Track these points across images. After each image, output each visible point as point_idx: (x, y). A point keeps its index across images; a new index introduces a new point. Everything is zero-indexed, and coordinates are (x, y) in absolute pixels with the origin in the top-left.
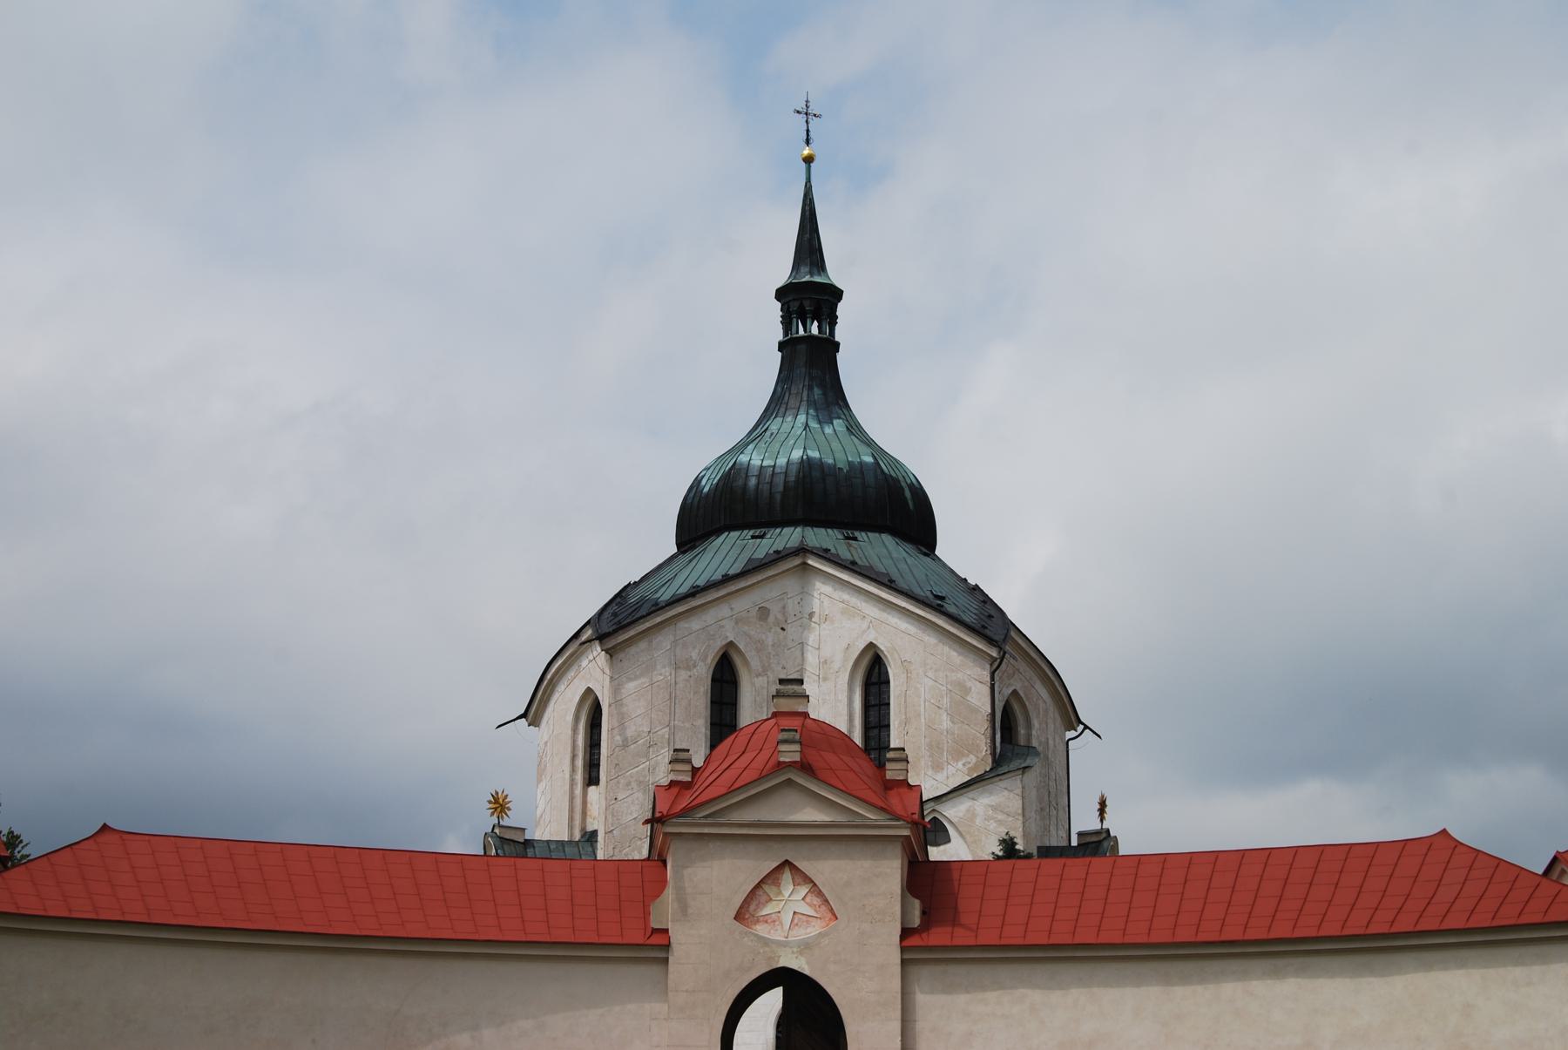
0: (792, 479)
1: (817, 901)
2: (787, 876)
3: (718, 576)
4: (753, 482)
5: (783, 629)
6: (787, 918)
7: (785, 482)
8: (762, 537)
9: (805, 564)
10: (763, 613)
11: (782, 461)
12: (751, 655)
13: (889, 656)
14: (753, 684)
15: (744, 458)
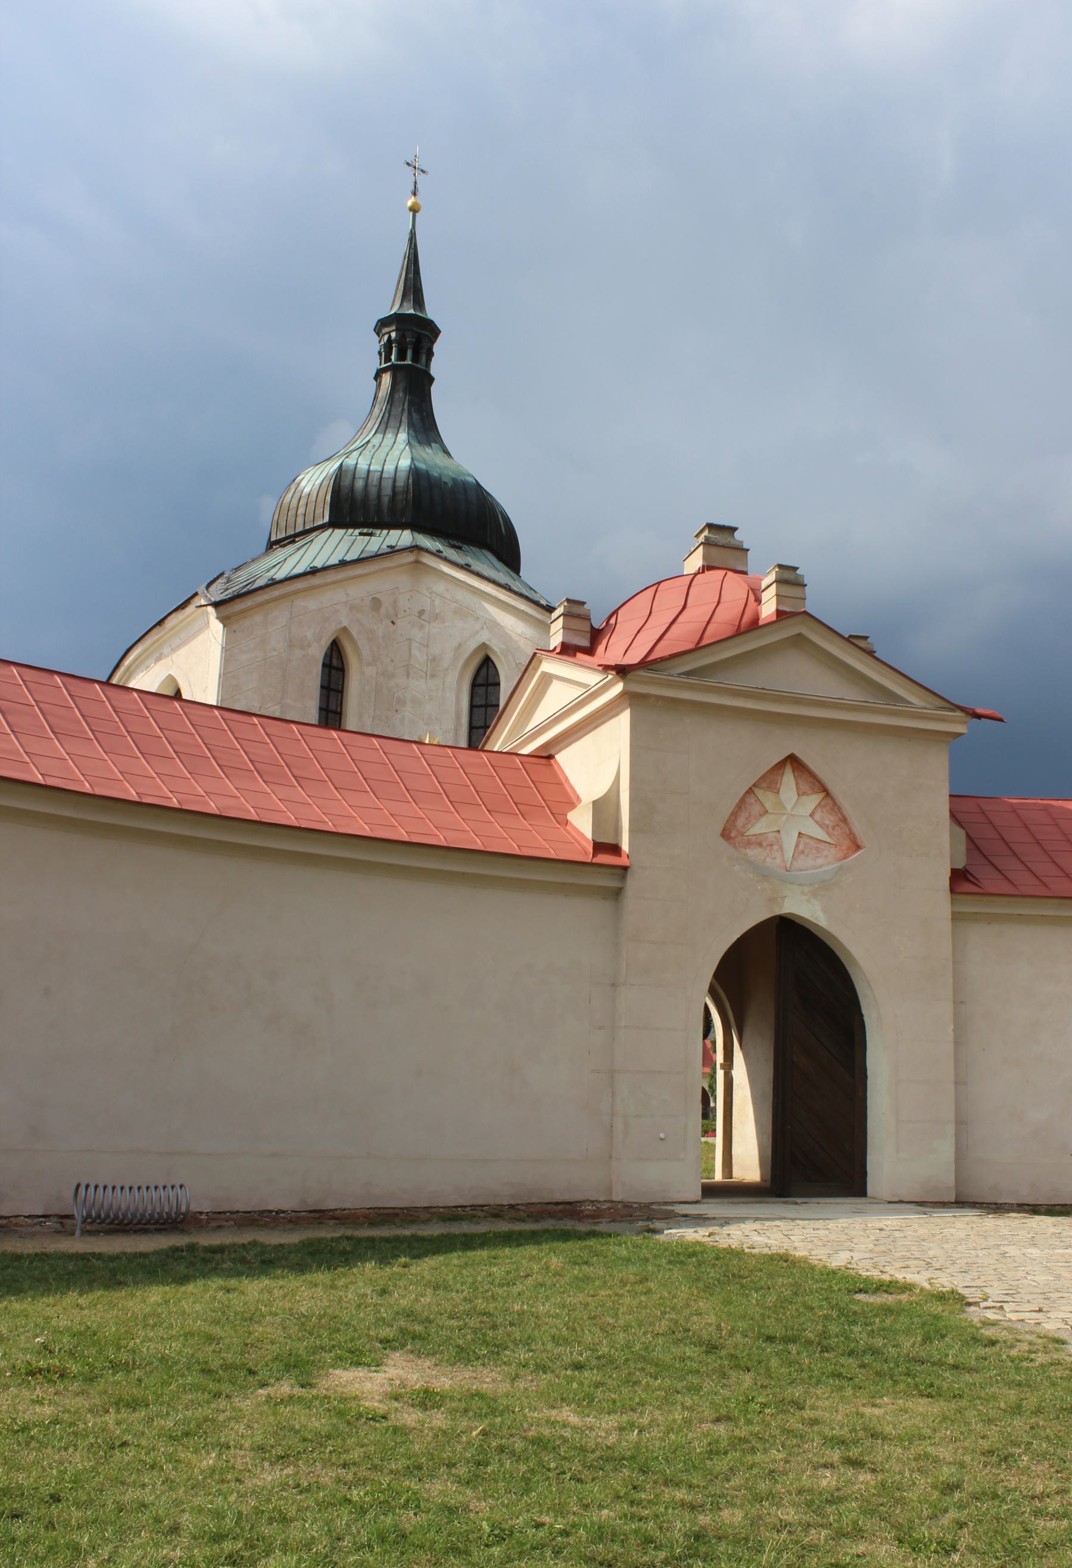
0: (400, 483)
1: (830, 819)
2: (788, 780)
3: (334, 560)
4: (360, 484)
5: (393, 623)
6: (789, 842)
7: (394, 487)
8: (371, 535)
9: (417, 562)
10: (376, 603)
11: (390, 468)
12: (362, 642)
13: (503, 658)
14: (363, 673)
15: (350, 462)
